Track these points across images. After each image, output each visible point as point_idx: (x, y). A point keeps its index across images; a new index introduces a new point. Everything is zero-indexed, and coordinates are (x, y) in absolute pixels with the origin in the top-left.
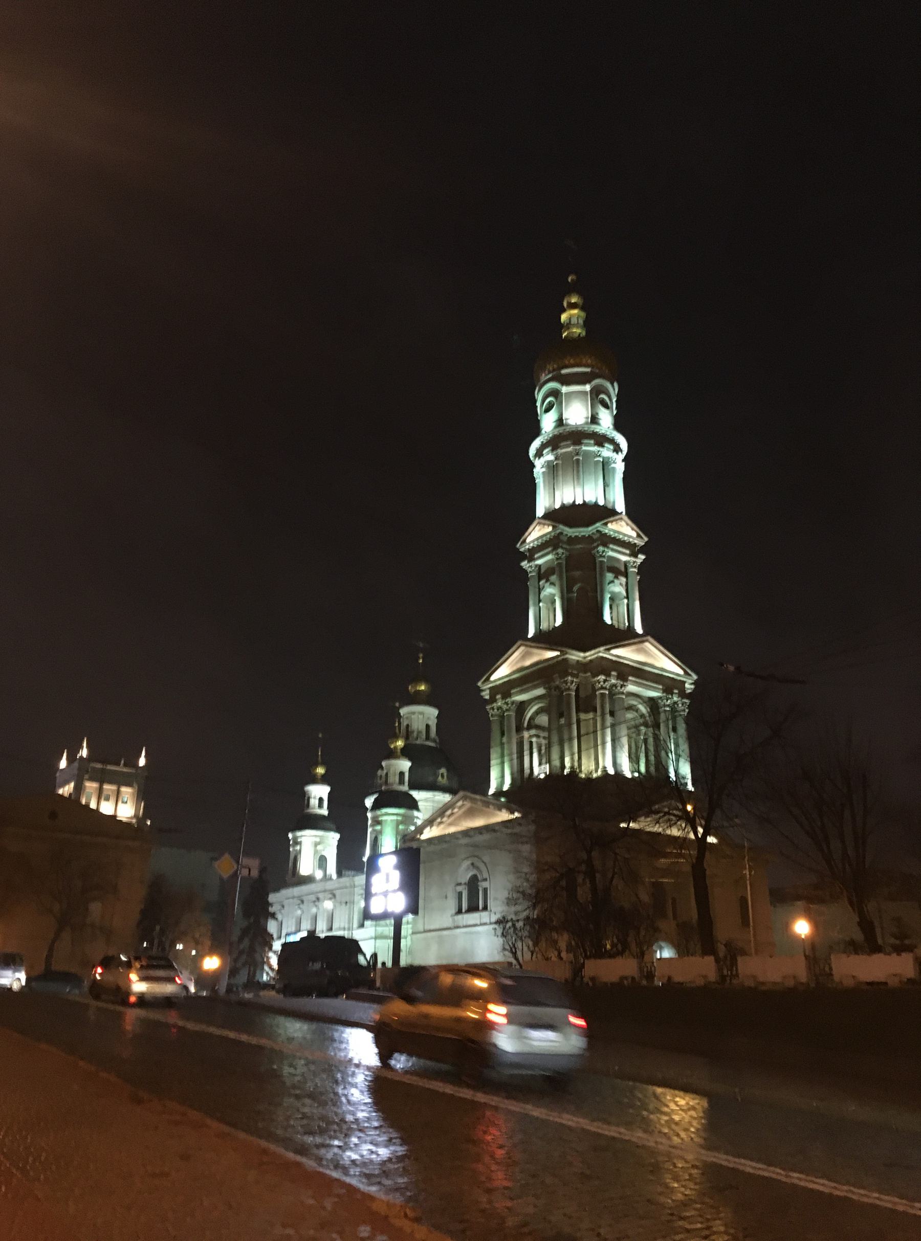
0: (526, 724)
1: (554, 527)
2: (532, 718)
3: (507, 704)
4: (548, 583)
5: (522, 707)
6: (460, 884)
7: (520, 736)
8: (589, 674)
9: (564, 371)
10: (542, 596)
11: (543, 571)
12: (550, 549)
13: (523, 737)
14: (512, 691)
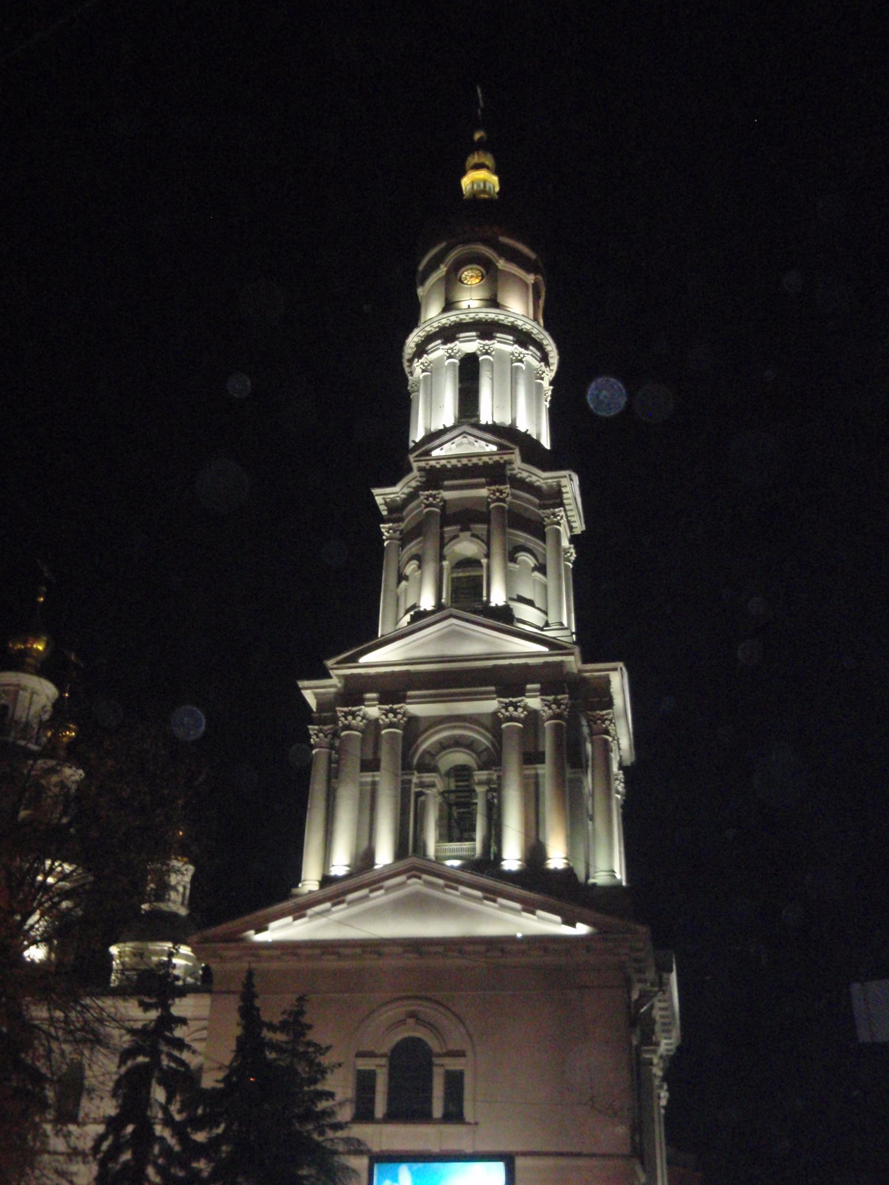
0: (415, 761)
1: (501, 447)
3: (395, 712)
4: (468, 534)
6: (371, 1055)
7: (408, 777)
9: (504, 240)
10: (447, 550)
11: (448, 512)
12: (483, 480)
13: (410, 781)
14: (410, 693)
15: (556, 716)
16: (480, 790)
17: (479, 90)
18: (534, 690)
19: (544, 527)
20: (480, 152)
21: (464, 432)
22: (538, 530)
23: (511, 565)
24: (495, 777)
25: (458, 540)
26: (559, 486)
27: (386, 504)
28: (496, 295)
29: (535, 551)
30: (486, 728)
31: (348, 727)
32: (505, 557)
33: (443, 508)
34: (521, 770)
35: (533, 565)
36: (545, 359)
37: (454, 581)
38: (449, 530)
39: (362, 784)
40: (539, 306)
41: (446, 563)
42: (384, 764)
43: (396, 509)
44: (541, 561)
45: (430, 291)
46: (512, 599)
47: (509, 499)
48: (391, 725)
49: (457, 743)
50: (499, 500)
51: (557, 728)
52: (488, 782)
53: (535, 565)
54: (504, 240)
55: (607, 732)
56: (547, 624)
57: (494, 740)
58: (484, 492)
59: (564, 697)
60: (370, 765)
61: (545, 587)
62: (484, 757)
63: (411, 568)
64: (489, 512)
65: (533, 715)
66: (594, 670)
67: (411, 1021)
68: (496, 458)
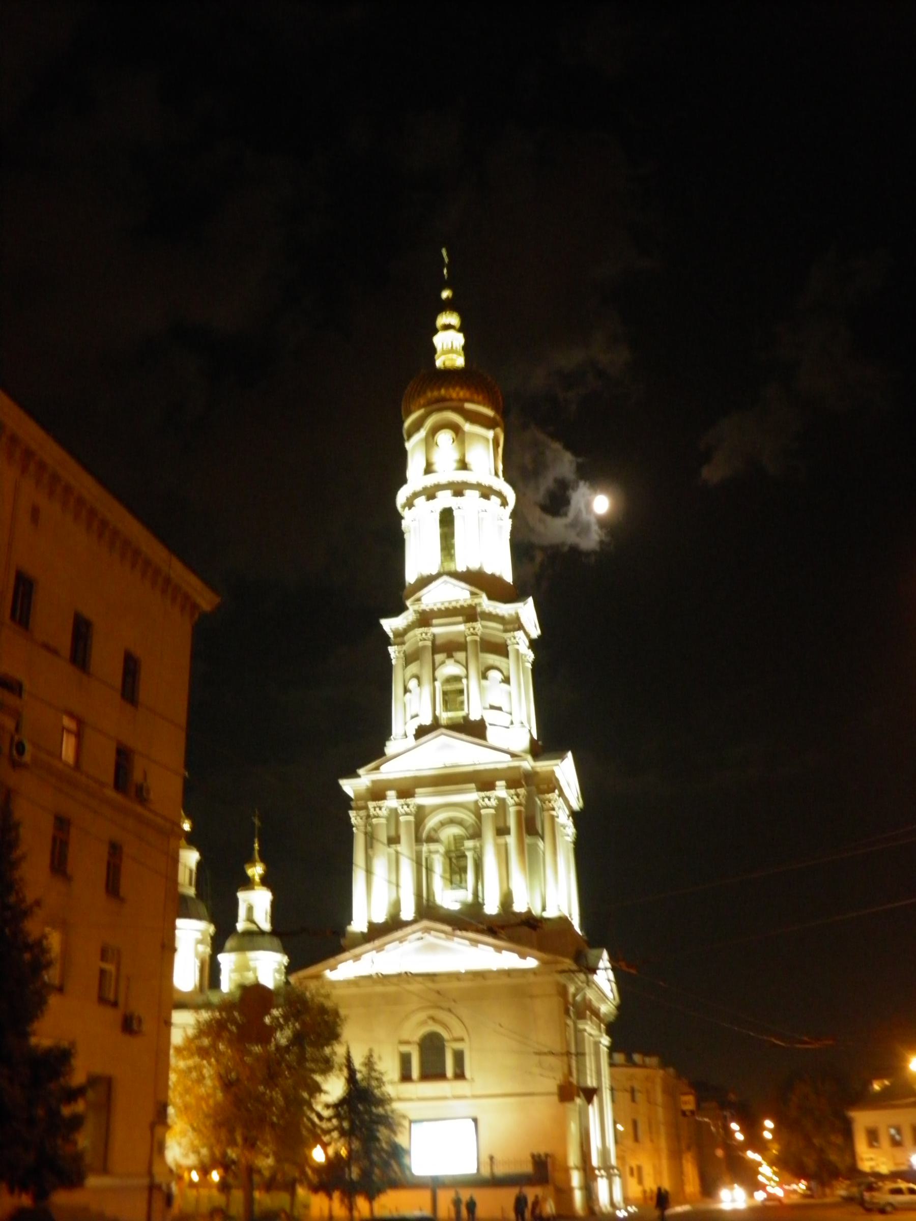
0: (424, 835)
1: (472, 594)
2: (435, 830)
5: (420, 815)
6: (407, 1043)
8: (534, 788)
9: (469, 406)
12: (460, 619)
14: (418, 790)
15: (517, 804)
16: (469, 854)
17: (444, 252)
18: (501, 786)
19: (507, 646)
20: (448, 312)
21: (445, 582)
22: (501, 650)
23: (484, 682)
24: (478, 845)
25: (444, 665)
26: (517, 614)
27: (392, 631)
28: (464, 456)
29: (501, 668)
30: (470, 810)
31: (377, 817)
32: (479, 675)
33: (433, 642)
34: (495, 840)
35: (500, 680)
36: (504, 503)
37: (445, 693)
38: (439, 657)
39: (389, 854)
40: (498, 452)
41: (438, 684)
42: (403, 838)
43: (401, 634)
44: (505, 673)
45: (414, 447)
46: (485, 708)
47: (479, 633)
48: (407, 814)
49: (452, 822)
50: (473, 634)
51: (519, 813)
52: (474, 849)
53: (502, 679)
54: (469, 406)
55: (553, 809)
56: (512, 723)
57: (477, 820)
58: (462, 627)
59: (522, 791)
60: (394, 840)
61: (510, 694)
62: (471, 831)
63: (413, 684)
64: (466, 642)
65: (502, 802)
66: (543, 766)
67: (430, 1022)
68: (469, 602)
